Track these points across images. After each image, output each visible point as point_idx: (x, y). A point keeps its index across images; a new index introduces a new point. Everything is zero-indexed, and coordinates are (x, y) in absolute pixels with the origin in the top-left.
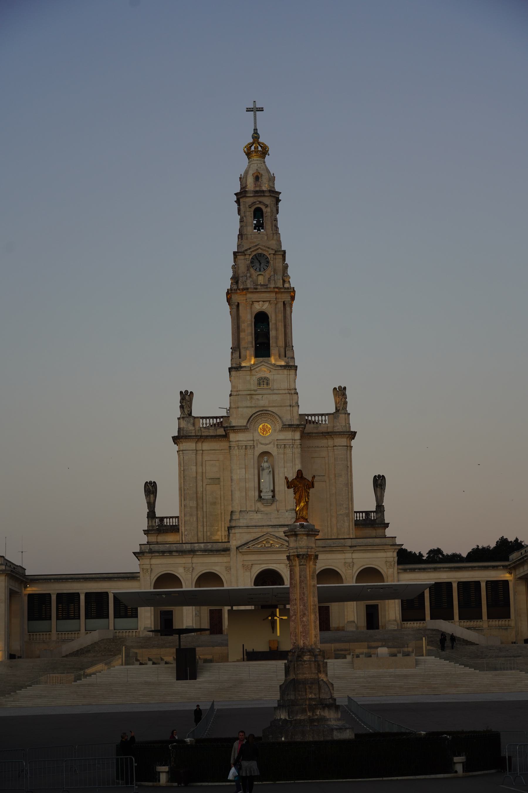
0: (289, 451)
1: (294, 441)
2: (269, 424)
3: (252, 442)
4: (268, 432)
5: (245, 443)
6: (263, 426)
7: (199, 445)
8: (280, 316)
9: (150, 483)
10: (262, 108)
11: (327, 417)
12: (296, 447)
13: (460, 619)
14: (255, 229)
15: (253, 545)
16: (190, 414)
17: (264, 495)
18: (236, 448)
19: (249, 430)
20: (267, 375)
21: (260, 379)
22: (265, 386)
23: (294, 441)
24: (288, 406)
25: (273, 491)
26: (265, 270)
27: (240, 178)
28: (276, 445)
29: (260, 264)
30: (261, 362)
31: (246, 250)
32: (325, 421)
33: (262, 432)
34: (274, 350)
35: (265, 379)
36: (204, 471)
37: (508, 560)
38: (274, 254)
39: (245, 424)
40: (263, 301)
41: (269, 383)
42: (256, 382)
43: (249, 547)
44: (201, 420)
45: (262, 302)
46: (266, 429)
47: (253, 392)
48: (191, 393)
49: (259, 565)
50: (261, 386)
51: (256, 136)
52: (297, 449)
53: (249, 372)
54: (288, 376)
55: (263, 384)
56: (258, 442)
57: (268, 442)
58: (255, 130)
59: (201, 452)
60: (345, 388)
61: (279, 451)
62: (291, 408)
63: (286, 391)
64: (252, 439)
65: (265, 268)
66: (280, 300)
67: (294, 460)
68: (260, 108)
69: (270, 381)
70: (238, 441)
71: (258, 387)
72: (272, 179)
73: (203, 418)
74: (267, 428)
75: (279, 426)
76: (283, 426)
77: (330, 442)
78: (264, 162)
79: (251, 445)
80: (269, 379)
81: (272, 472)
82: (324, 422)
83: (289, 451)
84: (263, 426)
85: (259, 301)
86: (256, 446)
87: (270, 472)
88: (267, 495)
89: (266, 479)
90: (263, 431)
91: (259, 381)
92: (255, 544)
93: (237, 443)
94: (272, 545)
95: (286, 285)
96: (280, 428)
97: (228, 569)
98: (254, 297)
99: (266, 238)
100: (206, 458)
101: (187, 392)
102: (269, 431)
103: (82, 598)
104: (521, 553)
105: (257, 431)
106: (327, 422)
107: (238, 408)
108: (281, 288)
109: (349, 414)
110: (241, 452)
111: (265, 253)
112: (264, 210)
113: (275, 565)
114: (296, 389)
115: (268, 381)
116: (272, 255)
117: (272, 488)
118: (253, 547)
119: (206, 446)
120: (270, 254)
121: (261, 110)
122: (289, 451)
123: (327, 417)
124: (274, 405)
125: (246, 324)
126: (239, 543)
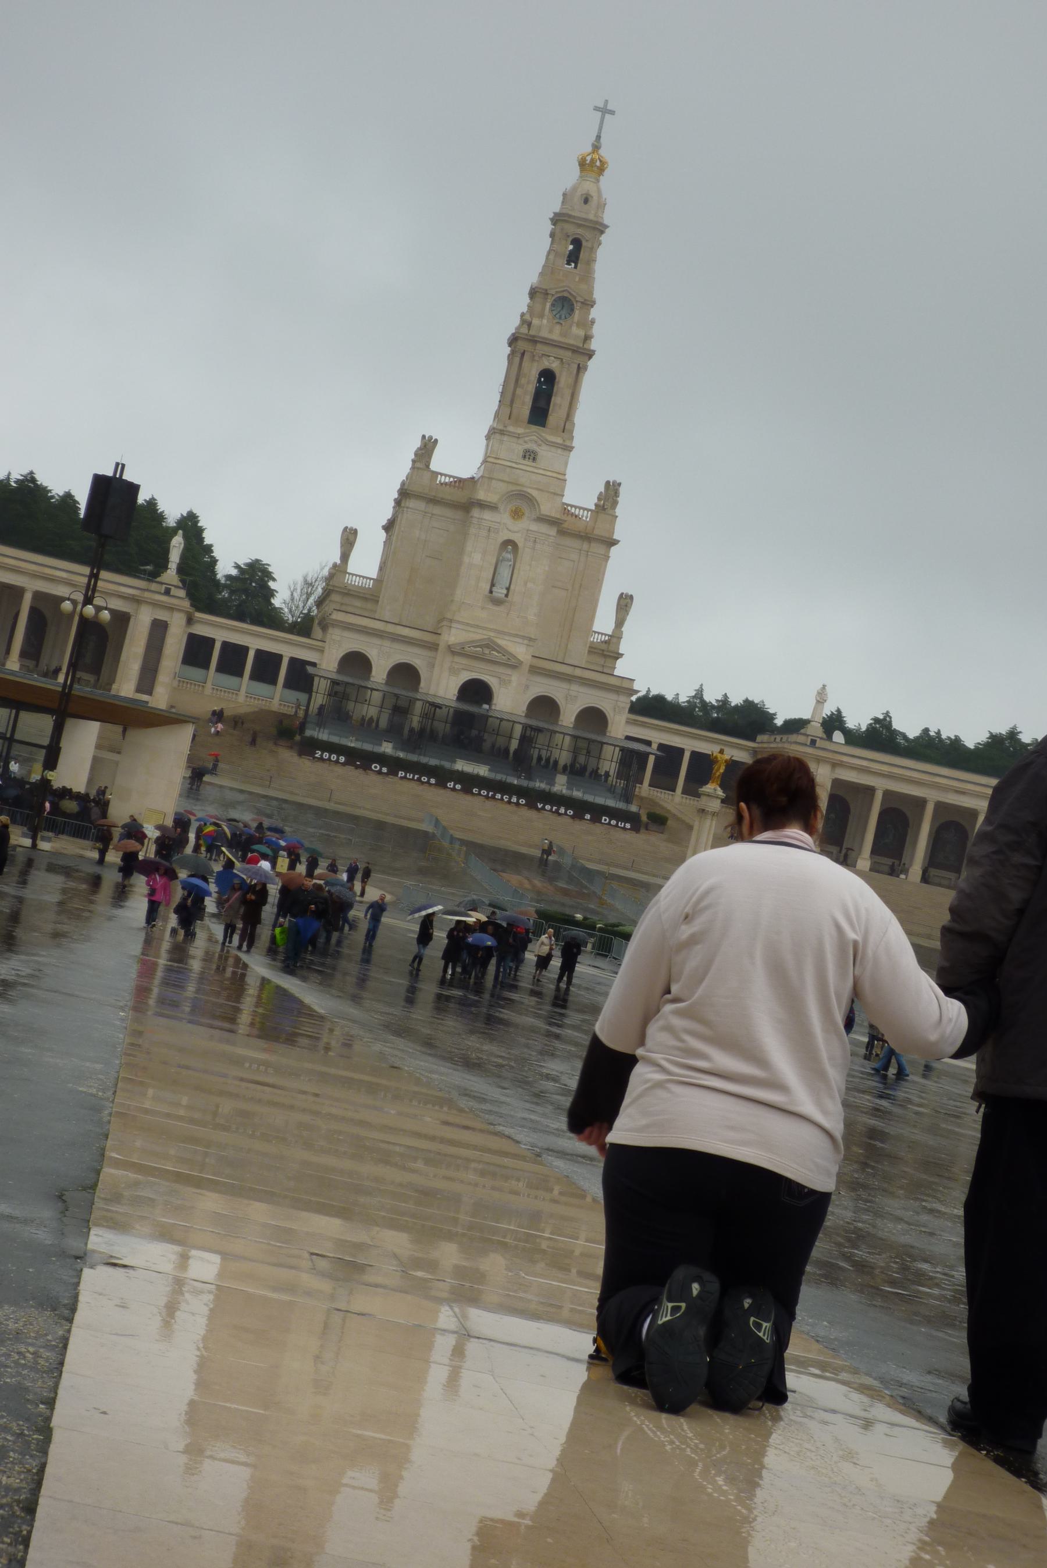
8: (571, 381)
9: (351, 529)
10: (614, 112)
11: (590, 513)
13: (682, 793)
14: (568, 263)
16: (428, 466)
25: (508, 589)
27: (564, 195)
29: (562, 308)
31: (550, 289)
32: (587, 518)
37: (753, 740)
38: (582, 303)
42: (521, 453)
44: (439, 476)
47: (514, 465)
48: (436, 441)
49: (469, 672)
51: (596, 147)
53: (515, 440)
55: (529, 458)
58: (598, 137)
59: (430, 515)
60: (619, 484)
63: (555, 475)
64: (499, 521)
65: (567, 316)
66: (575, 361)
68: (610, 111)
70: (482, 519)
72: (601, 206)
73: (442, 474)
77: (585, 546)
78: (598, 181)
82: (584, 518)
83: (538, 546)
84: (516, 508)
85: (549, 356)
87: (510, 565)
89: (505, 572)
95: (585, 346)
97: (431, 666)
98: (546, 349)
99: (577, 279)
101: (431, 438)
103: (251, 655)
104: (775, 739)
106: (588, 519)
107: (491, 479)
109: (617, 517)
111: (570, 297)
112: (584, 243)
113: (488, 677)
114: (565, 475)
117: (508, 585)
119: (437, 510)
120: (577, 301)
121: (612, 113)
123: (590, 513)
124: (535, 486)
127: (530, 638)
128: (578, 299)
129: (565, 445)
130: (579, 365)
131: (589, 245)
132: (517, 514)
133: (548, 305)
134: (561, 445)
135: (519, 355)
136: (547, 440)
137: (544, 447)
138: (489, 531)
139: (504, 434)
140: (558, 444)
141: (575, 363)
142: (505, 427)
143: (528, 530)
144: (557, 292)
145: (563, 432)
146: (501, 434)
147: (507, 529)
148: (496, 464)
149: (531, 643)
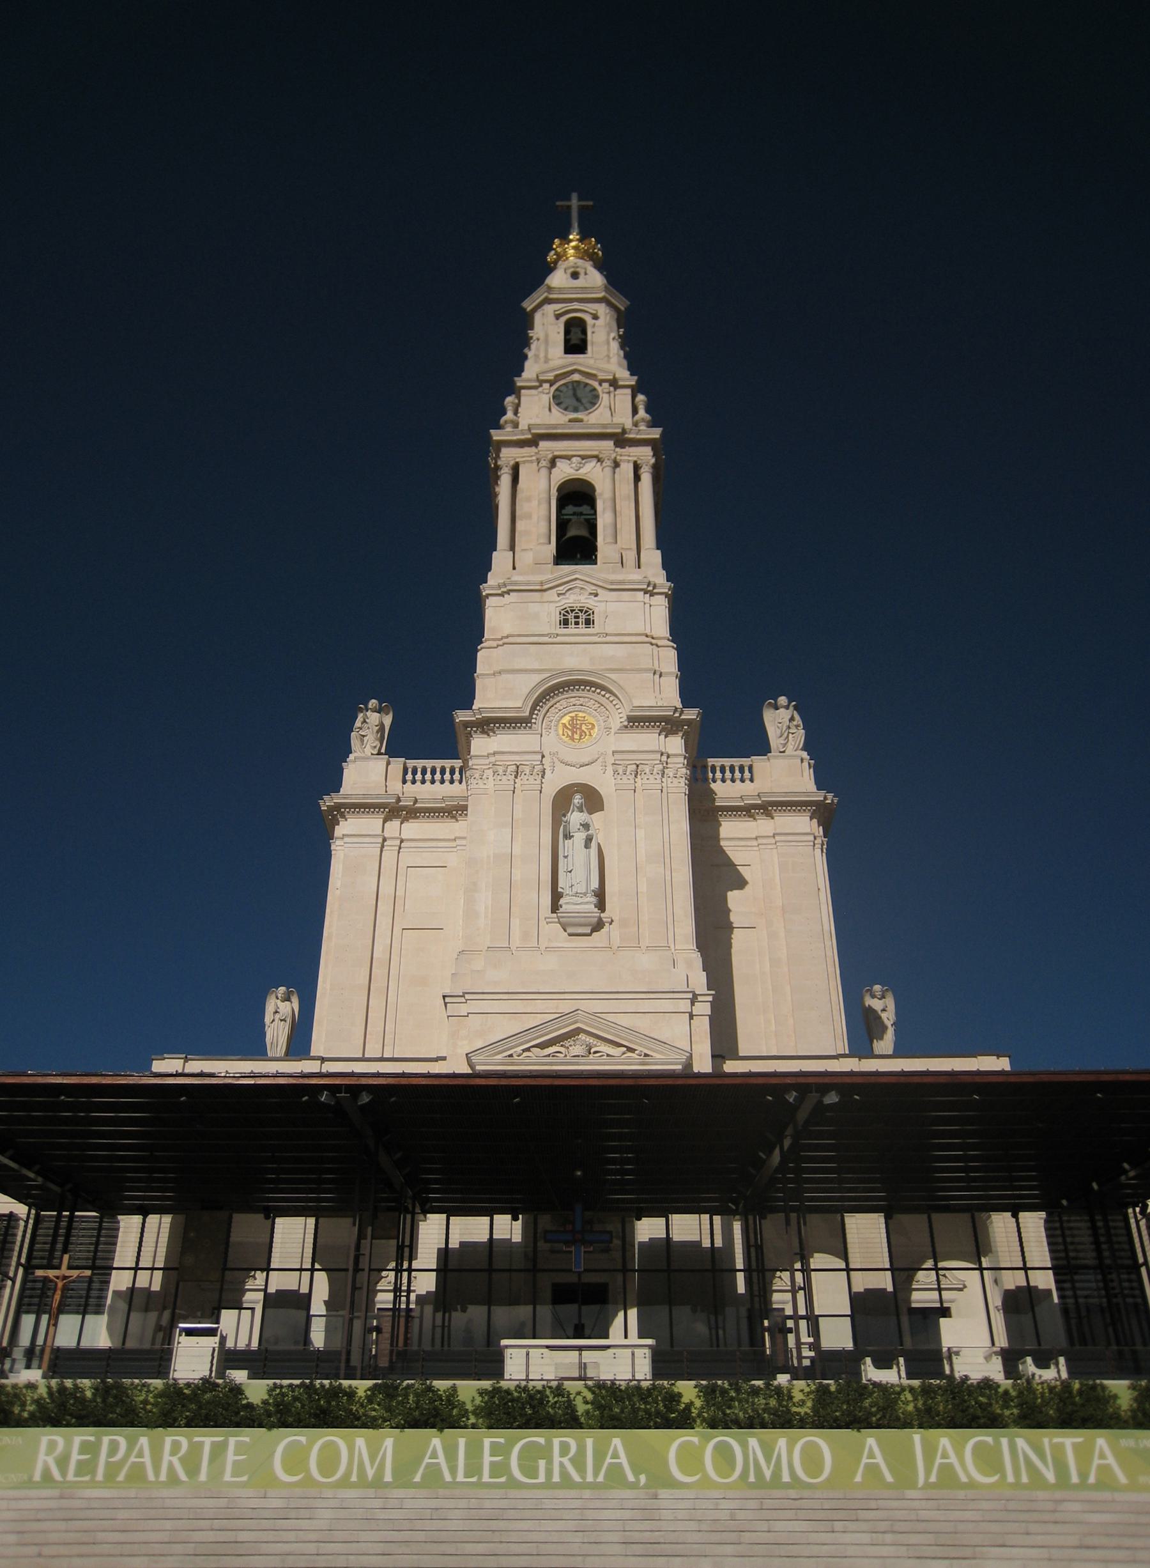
0: (652, 781)
1: (664, 758)
2: (589, 714)
4: (588, 733)
5: (517, 757)
7: (394, 824)
12: (671, 775)
15: (528, 1050)
17: (571, 901)
18: (490, 772)
20: (590, 602)
21: (567, 612)
22: (580, 626)
23: (664, 758)
24: (646, 670)
26: (587, 410)
28: (610, 769)
30: (574, 572)
33: (570, 733)
35: (581, 611)
36: (400, 893)
40: (583, 457)
41: (593, 620)
43: (511, 1056)
45: (579, 459)
47: (546, 639)
50: (570, 626)
54: (647, 606)
55: (577, 623)
56: (556, 760)
57: (586, 760)
61: (620, 782)
62: (657, 676)
67: (665, 809)
70: (494, 754)
74: (584, 727)
75: (618, 719)
76: (632, 711)
79: (535, 763)
83: (649, 781)
85: (569, 458)
88: (579, 905)
91: (564, 615)
93: (492, 759)
94: (592, 1051)
96: (625, 718)
100: (407, 858)
105: (552, 731)
115: (589, 615)
116: (606, 385)
117: (595, 884)
118: (526, 1054)
119: (412, 829)
122: (652, 781)
125: (535, 503)
128: (601, 376)
131: (598, 322)
132: (576, 730)
134: (640, 583)
136: (605, 581)
139: (508, 592)
140: (631, 582)
141: (629, 461)
143: (613, 752)
144: (558, 378)
145: (639, 567)
146: (502, 595)
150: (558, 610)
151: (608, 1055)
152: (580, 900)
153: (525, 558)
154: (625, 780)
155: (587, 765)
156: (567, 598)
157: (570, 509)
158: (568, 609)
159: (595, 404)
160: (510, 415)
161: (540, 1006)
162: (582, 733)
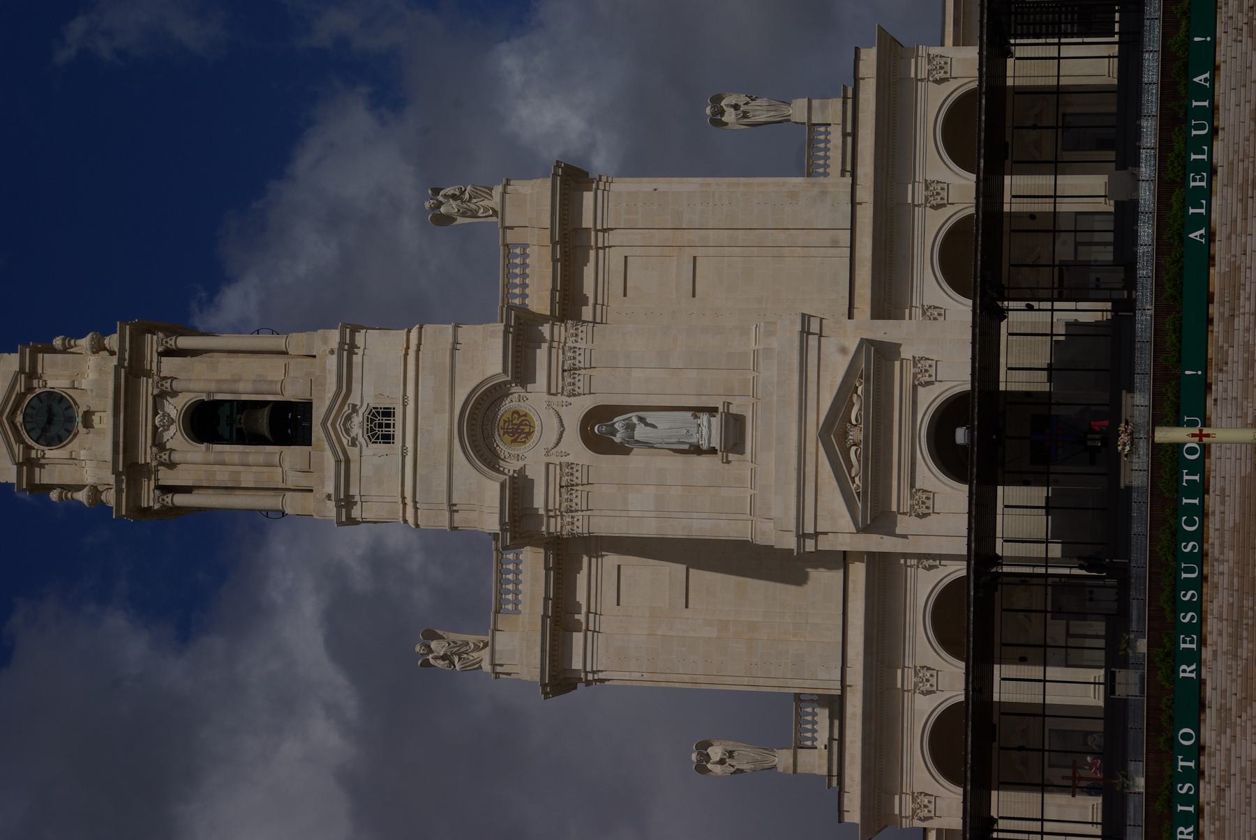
3: (551, 467)
4: (524, 418)
6: (508, 433)
19: (516, 475)
21: (373, 436)
22: (392, 422)
25: (696, 411)
26: (70, 407)
34: (292, 393)
35: (372, 421)
39: (497, 486)
40: (155, 413)
41: (384, 408)
42: (381, 447)
43: (858, 494)
45: (157, 420)
46: (515, 424)
50: (392, 433)
52: (580, 335)
55: (388, 426)
57: (555, 421)
62: (458, 347)
69: (379, 407)
71: (393, 443)
74: (515, 422)
80: (374, 408)
81: (642, 414)
83: (581, 360)
86: (564, 460)
87: (641, 419)
90: (521, 433)
91: (378, 438)
92: (850, 474)
102: (522, 416)
108: (121, 359)
110: (579, 504)
117: (689, 414)
118: (857, 479)
120: (30, 389)
126: (846, 523)
127: (802, 332)
128: (21, 387)
129: (341, 349)
130: (161, 354)
132: (521, 429)
133: (51, 453)
135: (168, 499)
137: (355, 399)
138: (571, 486)
141: (159, 362)
142: (329, 497)
144: (20, 440)
145: (314, 356)
147: (557, 444)
148: (415, 502)
149: (815, 327)
150: (371, 445)
151: (860, 410)
152: (705, 431)
153: (294, 479)
154: (580, 385)
155: (560, 417)
156: (357, 435)
157: (223, 429)
158: (369, 434)
159: (62, 397)
160: (82, 496)
161: (810, 468)
162: (521, 424)
